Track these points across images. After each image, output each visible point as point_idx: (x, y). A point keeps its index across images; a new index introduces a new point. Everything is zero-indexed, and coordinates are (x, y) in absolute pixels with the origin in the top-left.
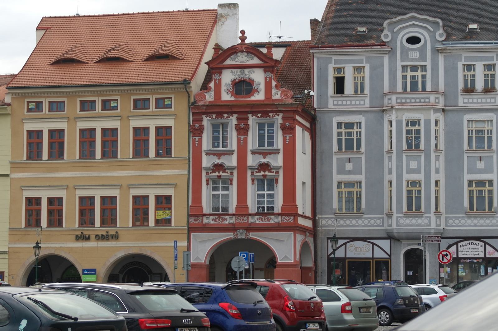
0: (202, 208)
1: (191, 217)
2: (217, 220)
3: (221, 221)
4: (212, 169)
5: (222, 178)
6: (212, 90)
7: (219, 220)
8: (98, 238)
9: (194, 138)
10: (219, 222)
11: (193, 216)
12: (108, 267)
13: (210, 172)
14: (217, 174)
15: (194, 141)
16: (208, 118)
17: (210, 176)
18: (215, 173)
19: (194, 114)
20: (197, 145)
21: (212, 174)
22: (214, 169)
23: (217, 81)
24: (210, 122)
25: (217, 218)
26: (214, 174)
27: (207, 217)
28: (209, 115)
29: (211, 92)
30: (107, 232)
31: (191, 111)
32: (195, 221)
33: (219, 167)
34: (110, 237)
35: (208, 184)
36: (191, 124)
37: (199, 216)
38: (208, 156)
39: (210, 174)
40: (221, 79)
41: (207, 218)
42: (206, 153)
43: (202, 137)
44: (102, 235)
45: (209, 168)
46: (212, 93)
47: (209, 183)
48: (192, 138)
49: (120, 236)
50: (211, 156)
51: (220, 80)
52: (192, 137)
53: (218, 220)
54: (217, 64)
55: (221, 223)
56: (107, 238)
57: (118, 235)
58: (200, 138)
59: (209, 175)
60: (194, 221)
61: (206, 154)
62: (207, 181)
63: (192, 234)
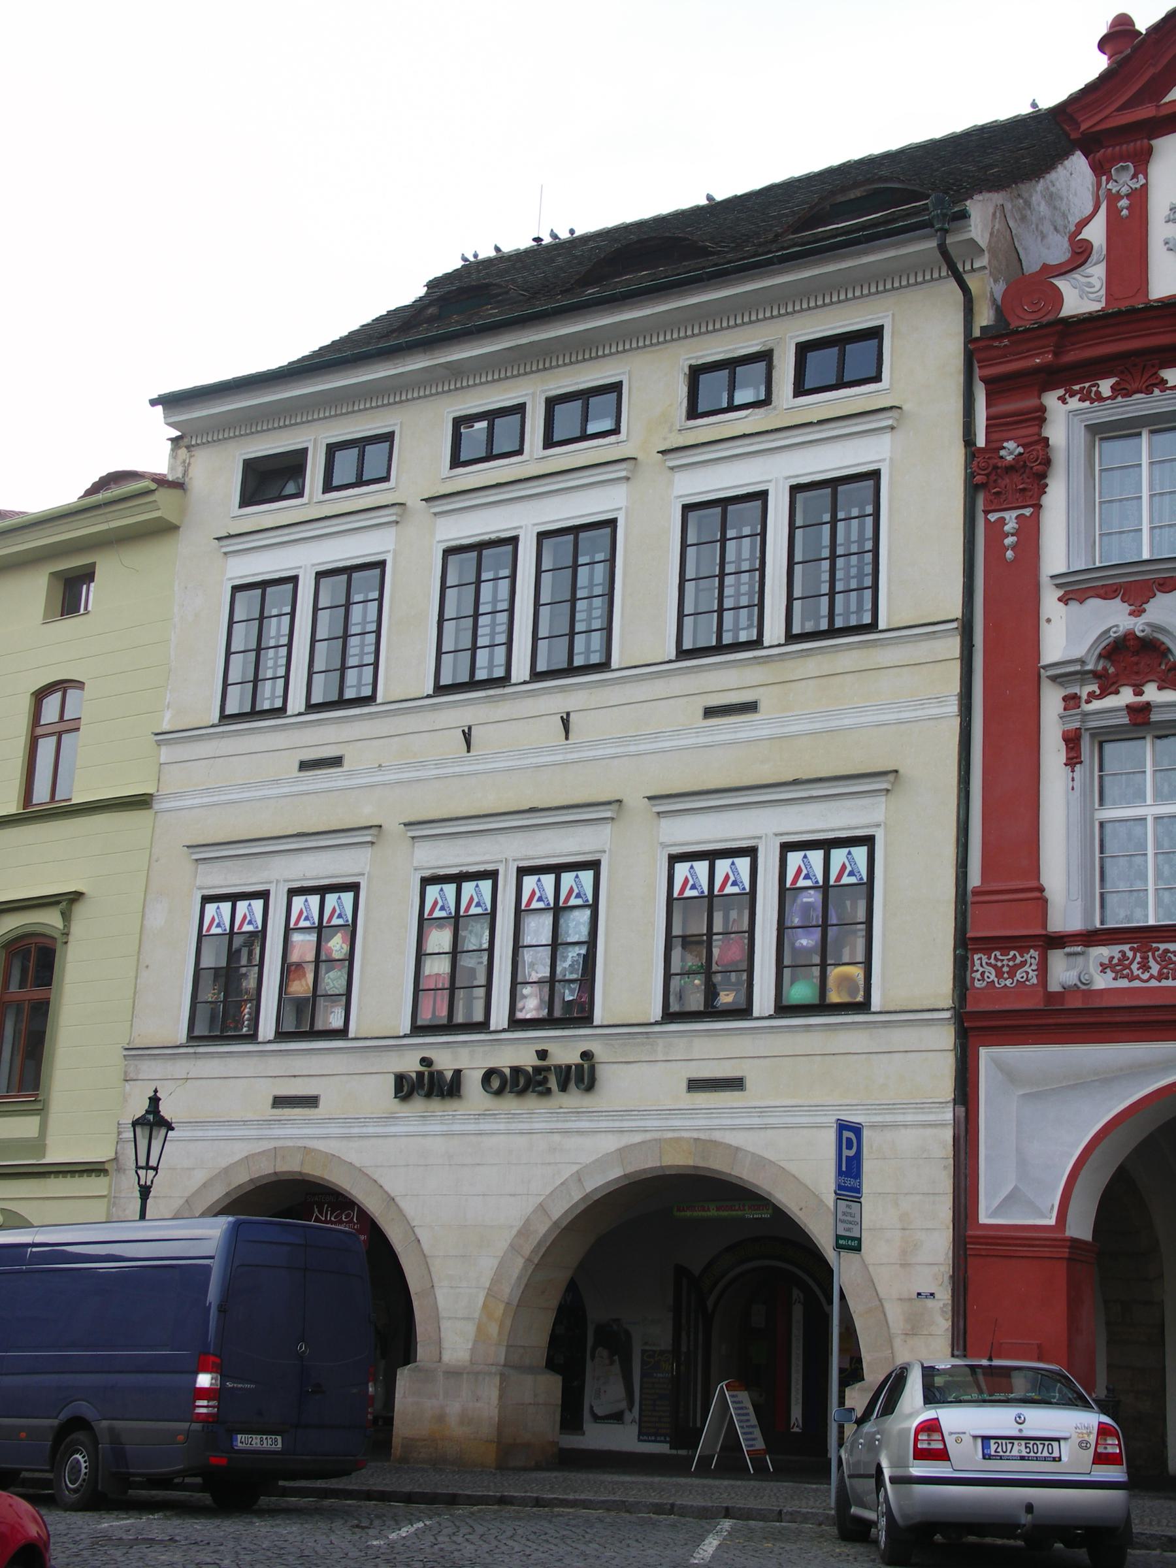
0: (1044, 901)
1: (977, 951)
2: (1129, 967)
3: (1155, 969)
4: (1096, 675)
5: (1154, 717)
6: (1094, 257)
7: (1145, 967)
8: (496, 1083)
9: (992, 517)
10: (1146, 976)
11: (988, 944)
12: (539, 1244)
13: (1084, 696)
14: (1126, 696)
15: (995, 531)
16: (1074, 403)
17: (1086, 714)
18: (1117, 692)
19: (997, 388)
20: (1009, 554)
21: (1096, 705)
22: (1111, 670)
23: (1124, 203)
24: (1082, 421)
25: (1130, 954)
26: (1110, 702)
27: (1067, 950)
28: (1077, 387)
29: (1090, 271)
30: (542, 1054)
31: (977, 372)
32: (999, 974)
33: (1135, 659)
34: (553, 1083)
35: (1073, 760)
36: (981, 442)
37: (1020, 943)
38: (1074, 605)
39: (1088, 702)
40: (1145, 187)
41: (1069, 955)
42: (1060, 593)
43: (1038, 507)
44: (516, 1071)
45: (1078, 668)
46: (1096, 272)
47: (1079, 756)
48: (987, 521)
49: (603, 1072)
50: (1094, 603)
51: (1140, 197)
52: (986, 512)
53: (1135, 966)
54: (1119, 109)
55: (1154, 983)
56: (540, 1083)
57: (592, 1069)
58: (1027, 512)
59: (1079, 707)
60: (993, 977)
61: (1064, 600)
62: (1072, 741)
63: (983, 1051)
